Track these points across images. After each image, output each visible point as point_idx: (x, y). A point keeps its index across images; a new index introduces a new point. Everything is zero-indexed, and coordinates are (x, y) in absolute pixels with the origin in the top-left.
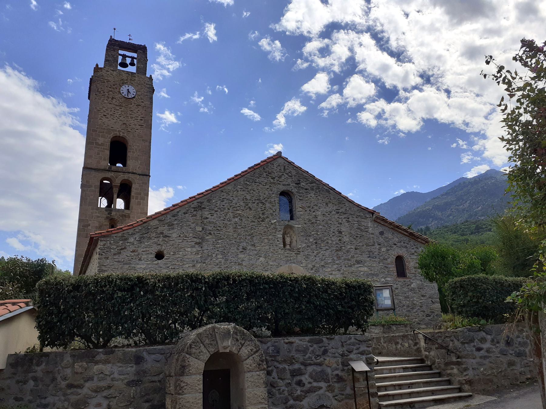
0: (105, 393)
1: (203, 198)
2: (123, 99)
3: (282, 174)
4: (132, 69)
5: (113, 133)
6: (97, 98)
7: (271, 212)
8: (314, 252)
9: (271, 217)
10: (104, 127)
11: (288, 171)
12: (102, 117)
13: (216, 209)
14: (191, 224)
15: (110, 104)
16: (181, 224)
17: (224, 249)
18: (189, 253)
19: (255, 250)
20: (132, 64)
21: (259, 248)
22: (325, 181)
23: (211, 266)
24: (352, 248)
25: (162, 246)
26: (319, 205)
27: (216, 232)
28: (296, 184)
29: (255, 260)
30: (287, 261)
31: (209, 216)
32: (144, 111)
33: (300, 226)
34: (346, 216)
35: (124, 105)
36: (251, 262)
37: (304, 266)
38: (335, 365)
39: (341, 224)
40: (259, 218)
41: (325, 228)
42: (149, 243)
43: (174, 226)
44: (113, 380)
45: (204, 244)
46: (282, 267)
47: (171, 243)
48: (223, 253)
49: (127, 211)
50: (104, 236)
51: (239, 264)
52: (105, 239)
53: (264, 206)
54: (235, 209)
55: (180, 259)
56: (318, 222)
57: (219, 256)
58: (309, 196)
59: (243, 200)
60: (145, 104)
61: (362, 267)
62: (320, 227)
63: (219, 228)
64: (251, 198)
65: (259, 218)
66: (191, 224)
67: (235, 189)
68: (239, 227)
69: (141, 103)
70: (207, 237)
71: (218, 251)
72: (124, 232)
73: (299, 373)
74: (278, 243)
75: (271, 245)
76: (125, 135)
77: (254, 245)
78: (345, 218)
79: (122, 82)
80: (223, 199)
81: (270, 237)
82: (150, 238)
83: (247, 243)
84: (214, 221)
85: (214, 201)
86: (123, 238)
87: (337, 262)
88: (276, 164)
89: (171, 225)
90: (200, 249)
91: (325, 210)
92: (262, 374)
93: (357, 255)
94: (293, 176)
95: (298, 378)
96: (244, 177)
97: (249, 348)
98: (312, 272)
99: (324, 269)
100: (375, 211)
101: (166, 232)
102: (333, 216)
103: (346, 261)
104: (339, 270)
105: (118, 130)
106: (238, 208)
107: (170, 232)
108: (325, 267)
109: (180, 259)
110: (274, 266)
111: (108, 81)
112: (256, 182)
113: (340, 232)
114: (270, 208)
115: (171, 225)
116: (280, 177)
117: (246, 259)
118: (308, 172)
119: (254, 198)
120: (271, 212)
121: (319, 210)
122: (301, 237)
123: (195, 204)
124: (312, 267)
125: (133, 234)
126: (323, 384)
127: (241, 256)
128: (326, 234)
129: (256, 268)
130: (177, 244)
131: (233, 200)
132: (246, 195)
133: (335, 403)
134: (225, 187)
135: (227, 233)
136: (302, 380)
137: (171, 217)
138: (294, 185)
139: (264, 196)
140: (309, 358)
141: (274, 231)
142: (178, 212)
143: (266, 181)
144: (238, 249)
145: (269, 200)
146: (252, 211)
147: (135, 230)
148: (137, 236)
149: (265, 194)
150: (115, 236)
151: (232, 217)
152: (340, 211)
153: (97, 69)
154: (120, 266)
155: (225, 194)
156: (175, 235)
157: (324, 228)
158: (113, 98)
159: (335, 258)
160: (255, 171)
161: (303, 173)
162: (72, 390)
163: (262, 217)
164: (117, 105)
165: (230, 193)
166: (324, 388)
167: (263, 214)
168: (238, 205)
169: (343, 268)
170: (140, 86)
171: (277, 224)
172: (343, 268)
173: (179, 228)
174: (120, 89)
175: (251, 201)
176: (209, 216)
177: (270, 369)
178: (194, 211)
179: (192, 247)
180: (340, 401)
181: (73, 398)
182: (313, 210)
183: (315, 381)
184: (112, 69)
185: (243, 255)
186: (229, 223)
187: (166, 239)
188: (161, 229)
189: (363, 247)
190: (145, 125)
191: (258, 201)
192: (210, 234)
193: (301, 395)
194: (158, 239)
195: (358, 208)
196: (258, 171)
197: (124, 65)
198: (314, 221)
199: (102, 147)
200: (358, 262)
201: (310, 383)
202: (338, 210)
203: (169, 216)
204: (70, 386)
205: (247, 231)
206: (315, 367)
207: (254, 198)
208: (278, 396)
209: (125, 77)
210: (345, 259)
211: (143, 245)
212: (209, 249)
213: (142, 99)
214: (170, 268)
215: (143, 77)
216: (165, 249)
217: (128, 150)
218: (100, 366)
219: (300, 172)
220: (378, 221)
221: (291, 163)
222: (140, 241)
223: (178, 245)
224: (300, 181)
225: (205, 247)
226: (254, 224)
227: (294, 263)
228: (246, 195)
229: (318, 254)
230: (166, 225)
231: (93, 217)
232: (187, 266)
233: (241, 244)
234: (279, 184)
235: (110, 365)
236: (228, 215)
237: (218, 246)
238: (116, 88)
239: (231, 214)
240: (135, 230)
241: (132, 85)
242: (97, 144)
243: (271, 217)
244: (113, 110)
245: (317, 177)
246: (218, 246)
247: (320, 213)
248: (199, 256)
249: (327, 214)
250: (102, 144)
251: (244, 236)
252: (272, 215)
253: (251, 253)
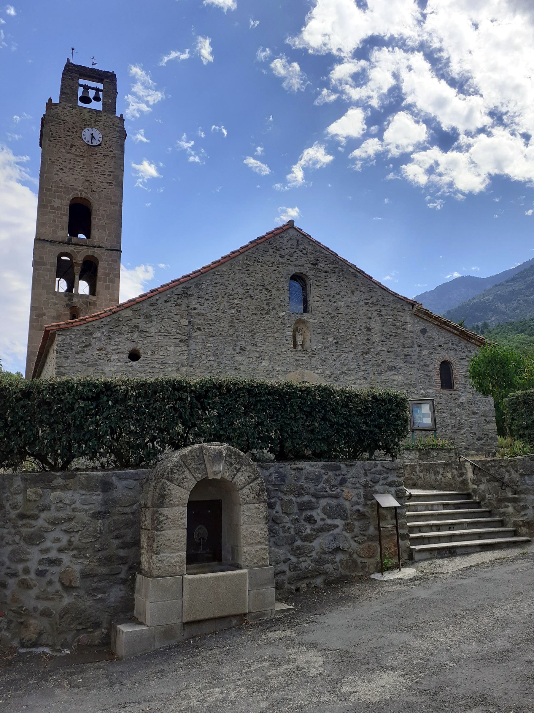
0: (64, 527)
1: (189, 282)
2: (86, 147)
3: (294, 250)
4: (97, 106)
5: (73, 193)
6: (52, 145)
7: (279, 302)
8: (333, 355)
9: (278, 309)
10: (61, 185)
11: (302, 247)
12: (58, 171)
13: (207, 297)
14: (174, 316)
15: (69, 153)
16: (161, 316)
17: (217, 349)
18: (172, 353)
19: (257, 351)
20: (97, 99)
21: (261, 348)
22: (351, 260)
23: (199, 370)
24: (383, 350)
25: (137, 343)
26: (342, 293)
27: (206, 328)
28: (312, 264)
30: (299, 366)
31: (198, 306)
32: (112, 164)
33: (316, 321)
34: (376, 308)
35: (86, 155)
36: (252, 366)
37: (320, 372)
38: (355, 499)
39: (371, 318)
40: (262, 310)
41: (349, 324)
42: (121, 339)
43: (152, 318)
44: (74, 510)
45: (191, 342)
46: (291, 374)
47: (149, 339)
48: (215, 354)
49: (93, 298)
50: (63, 329)
51: (236, 369)
52: (64, 333)
53: (269, 294)
54: (231, 297)
55: (160, 360)
56: (340, 315)
57: (210, 358)
58: (329, 280)
59: (242, 285)
60: (114, 154)
61: (396, 374)
62: (343, 322)
63: (210, 322)
64: (252, 283)
65: (262, 310)
66: (174, 316)
67: (231, 271)
68: (236, 321)
69: (110, 153)
70: (196, 334)
71: (209, 351)
72: (88, 324)
73: (309, 506)
74: (287, 342)
75: (278, 345)
76: (89, 195)
77: (255, 345)
78: (376, 311)
79: (83, 123)
80: (216, 283)
81: (277, 335)
82: (121, 333)
83: (246, 341)
84: (204, 312)
85: (203, 286)
86: (88, 332)
87: (363, 368)
88: (286, 236)
89: (148, 317)
90: (186, 349)
91: (350, 300)
92: (262, 507)
93: (390, 360)
94: (309, 254)
95: (308, 513)
96: (243, 255)
97: (246, 474)
98: (329, 380)
99: (346, 377)
100: (416, 302)
101: (142, 326)
102: (360, 308)
103: (375, 367)
104: (365, 379)
105: (79, 189)
106: (236, 296)
107: (148, 326)
108: (346, 374)
109: (160, 360)
110: (281, 372)
111: (66, 122)
112: (259, 262)
113: (369, 330)
114: (278, 297)
115: (148, 317)
116: (291, 255)
117: (244, 362)
118: (328, 249)
119: (257, 283)
120: (279, 302)
121: (342, 300)
122: (318, 335)
123: (180, 290)
124: (330, 374)
125: (99, 327)
126: (339, 522)
127: (239, 358)
128: (350, 331)
129: (258, 375)
130: (156, 341)
131: (229, 285)
132: (246, 279)
133: (354, 545)
134: (218, 268)
135: (221, 329)
136: (312, 516)
137: (148, 307)
138: (310, 266)
139: (270, 280)
140: (323, 488)
141: (282, 327)
142: (157, 300)
143: (272, 260)
144: (235, 350)
145: (276, 286)
146: (254, 301)
147: (102, 322)
148: (105, 330)
149: (271, 278)
150: (77, 330)
151: (227, 307)
152: (370, 301)
153: (50, 105)
154: (84, 368)
155: (218, 277)
156: (153, 330)
157: (347, 324)
158: (72, 146)
159: (361, 363)
160: (258, 246)
161: (322, 249)
162: (25, 521)
163: (267, 308)
164: (77, 156)
165: (224, 276)
166: (341, 527)
167: (268, 304)
168: (235, 292)
169: (371, 375)
170: (107, 129)
171: (286, 318)
172: (371, 375)
173: (159, 321)
174: (81, 133)
175: (252, 287)
176: (198, 306)
177: (273, 501)
178: (178, 299)
179: (176, 345)
180: (360, 543)
181: (26, 531)
182: (333, 300)
183: (330, 517)
184: (70, 105)
185: (242, 358)
186: (223, 315)
187: (143, 335)
188: (135, 321)
189: (398, 349)
190: (114, 183)
191: (261, 288)
192: (199, 329)
193: (311, 535)
194: (131, 334)
195: (393, 298)
196: (262, 246)
197: (86, 99)
198: (334, 314)
199: (59, 212)
200: (391, 369)
201: (323, 519)
202: (367, 300)
203: (145, 305)
204: (22, 516)
205: (247, 326)
206: (329, 500)
207: (257, 283)
208: (282, 534)
209: (87, 116)
210: (373, 365)
211: (113, 342)
212: (197, 348)
213: (110, 147)
214: (148, 371)
215: (111, 116)
216: (142, 347)
217: (93, 216)
218: (58, 493)
219: (318, 248)
220: (420, 315)
221: (306, 237)
222: (109, 337)
223: (158, 342)
224: (317, 260)
225: (192, 346)
226: (255, 317)
227: (307, 368)
228: (246, 279)
229: (338, 357)
230: (142, 317)
231: (48, 304)
232: (170, 369)
233: (240, 343)
234: (289, 264)
235: (70, 492)
236: (222, 305)
237: (209, 345)
238: (77, 132)
239: (226, 304)
240: (102, 322)
241: (97, 127)
242: (53, 207)
243: (278, 309)
244: (72, 161)
245: (341, 255)
246: (209, 345)
247: (342, 304)
248: (185, 358)
249: (352, 305)
250: (59, 208)
251: (242, 332)
252: (280, 306)
253: (251, 356)
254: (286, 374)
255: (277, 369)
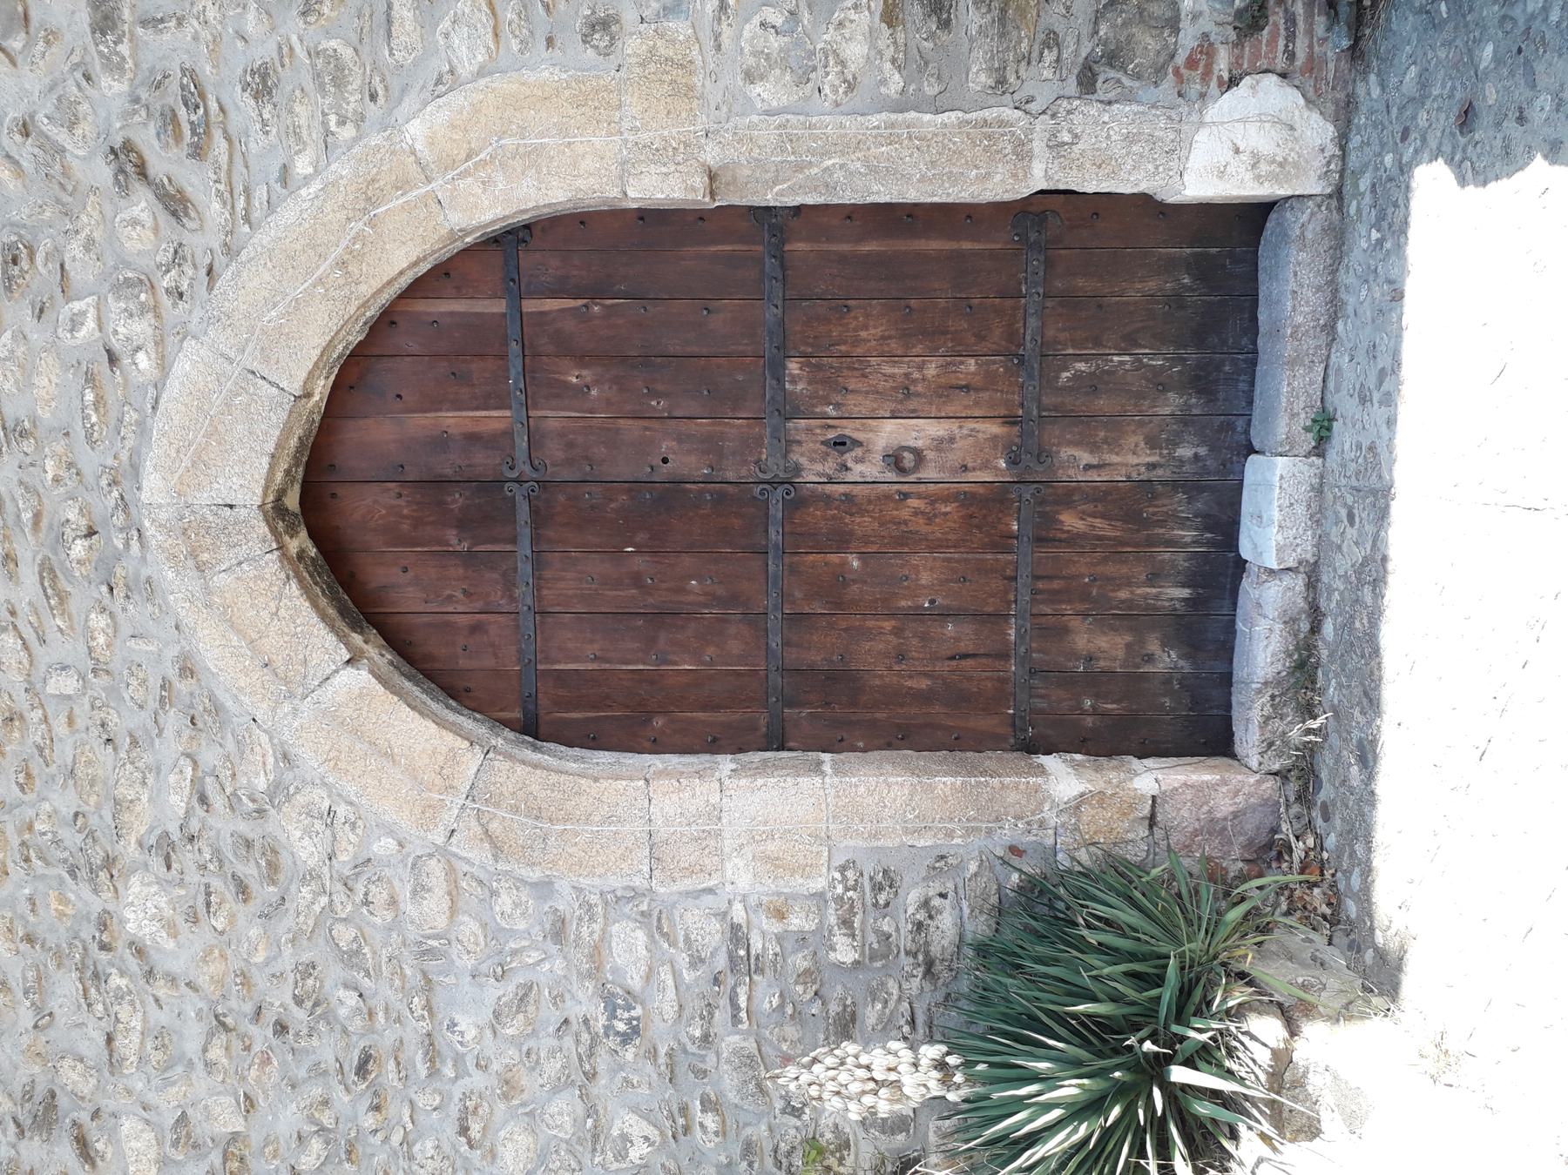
19: (38, 987)
29: (162, 990)
98: (215, 210)
110: (210, 757)
117: (168, 1103)
129: (260, 981)
185: (128, 1126)
227: (125, 476)
254: (217, 709)
255: (178, 802)
